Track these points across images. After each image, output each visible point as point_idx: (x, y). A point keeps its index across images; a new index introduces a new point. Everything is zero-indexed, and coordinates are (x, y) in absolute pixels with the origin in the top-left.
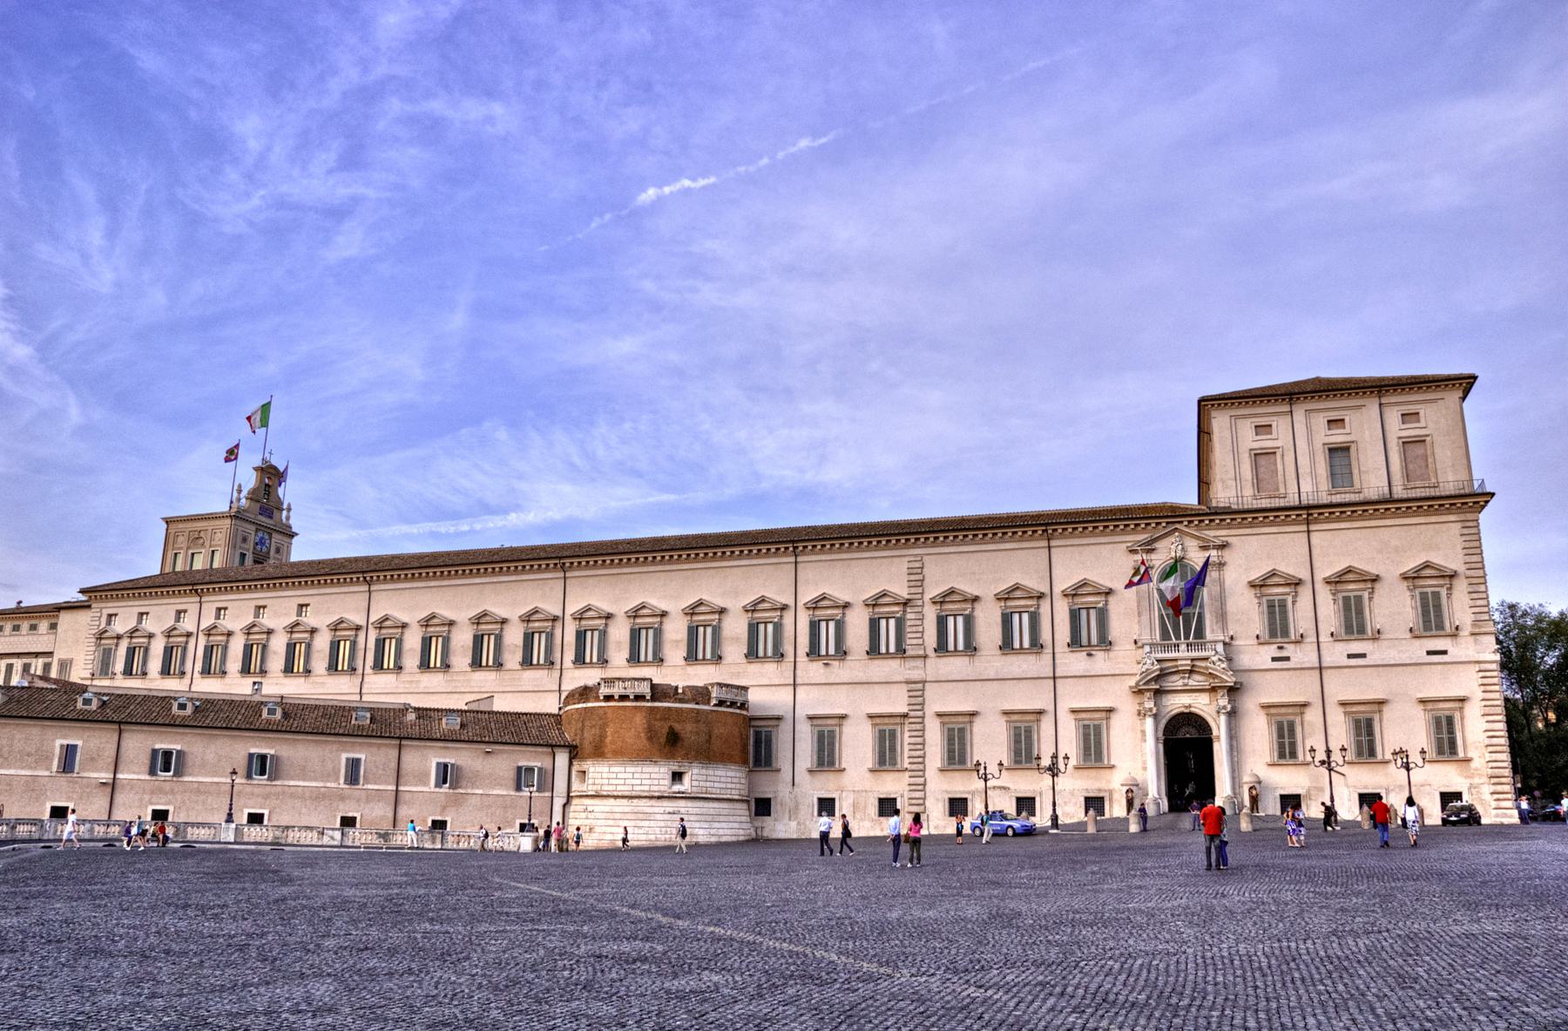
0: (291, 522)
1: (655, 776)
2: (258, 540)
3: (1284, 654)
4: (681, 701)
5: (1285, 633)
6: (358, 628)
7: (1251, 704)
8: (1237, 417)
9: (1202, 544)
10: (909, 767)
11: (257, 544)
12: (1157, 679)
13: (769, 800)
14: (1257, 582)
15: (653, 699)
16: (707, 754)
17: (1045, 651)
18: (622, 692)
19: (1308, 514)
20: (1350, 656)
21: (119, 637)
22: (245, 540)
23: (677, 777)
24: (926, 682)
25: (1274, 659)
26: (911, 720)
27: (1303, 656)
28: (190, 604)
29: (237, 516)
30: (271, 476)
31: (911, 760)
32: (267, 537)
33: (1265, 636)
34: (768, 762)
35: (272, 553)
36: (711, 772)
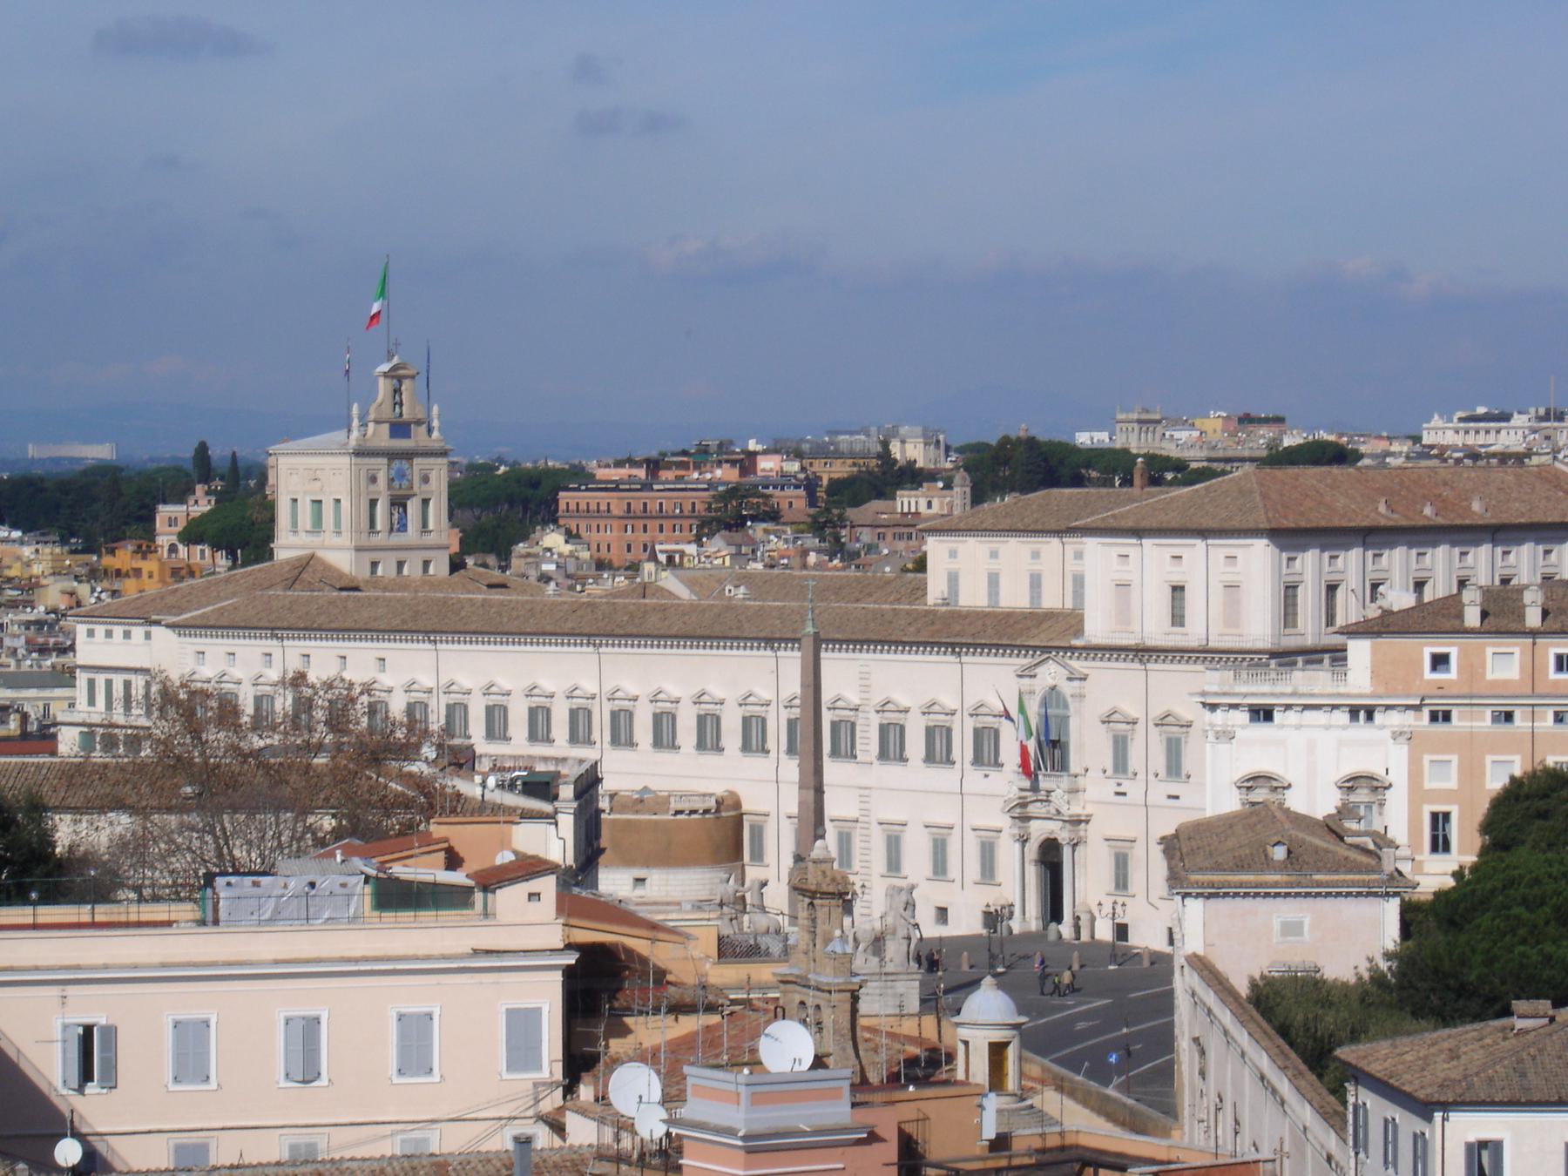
2: (393, 473)
3: (1121, 789)
5: (1125, 771)
7: (1093, 832)
10: (861, 871)
11: (393, 480)
12: (1023, 805)
17: (956, 765)
19: (1142, 653)
20: (1170, 797)
22: (373, 480)
24: (870, 788)
25: (1118, 794)
26: (862, 825)
27: (1134, 789)
31: (864, 864)
32: (407, 466)
33: (1110, 772)
36: (671, 877)
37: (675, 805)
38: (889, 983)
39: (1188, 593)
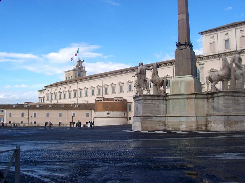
0: (85, 70)
1: (105, 114)
4: (108, 101)
6: (76, 90)
8: (207, 35)
9: (200, 64)
13: (131, 117)
14: (209, 71)
15: (103, 101)
16: (113, 109)
18: (99, 100)
21: (49, 94)
22: (76, 74)
23: (108, 114)
28: (56, 88)
29: (74, 70)
30: (80, 62)
34: (131, 111)
35: (82, 75)
36: (114, 113)
37: (115, 99)
38: (236, 98)
39: (231, 41)
